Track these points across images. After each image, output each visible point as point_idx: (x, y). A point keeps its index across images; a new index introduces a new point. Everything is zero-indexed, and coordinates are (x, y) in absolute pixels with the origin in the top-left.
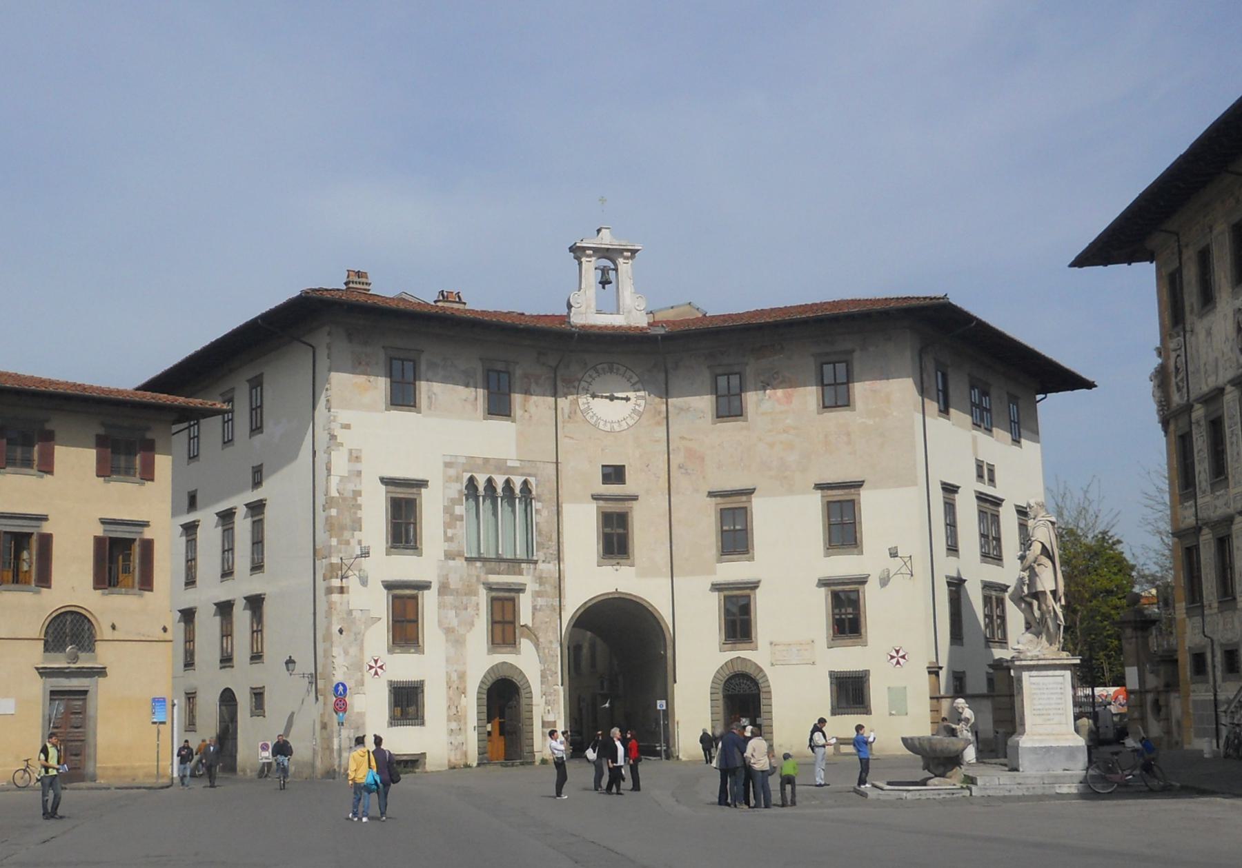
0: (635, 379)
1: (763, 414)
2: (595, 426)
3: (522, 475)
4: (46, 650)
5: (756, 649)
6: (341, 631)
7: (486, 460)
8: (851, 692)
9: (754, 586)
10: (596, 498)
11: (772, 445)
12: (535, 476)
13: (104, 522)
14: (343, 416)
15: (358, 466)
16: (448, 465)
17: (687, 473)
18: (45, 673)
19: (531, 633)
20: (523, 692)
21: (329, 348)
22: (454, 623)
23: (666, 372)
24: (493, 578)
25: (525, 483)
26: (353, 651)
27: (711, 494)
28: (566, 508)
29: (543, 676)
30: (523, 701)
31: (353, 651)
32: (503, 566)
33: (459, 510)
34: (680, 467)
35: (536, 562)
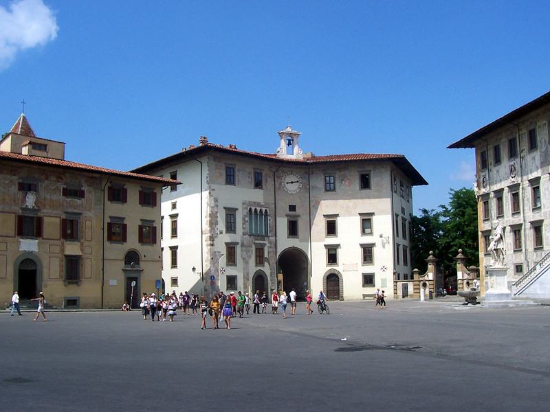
4: (125, 264)
8: (368, 280)
10: (287, 216)
13: (141, 220)
14: (213, 186)
16: (243, 204)
18: (124, 271)
20: (265, 279)
21: (208, 163)
22: (246, 256)
24: (257, 242)
28: (278, 219)
30: (265, 282)
32: (259, 238)
33: (247, 219)
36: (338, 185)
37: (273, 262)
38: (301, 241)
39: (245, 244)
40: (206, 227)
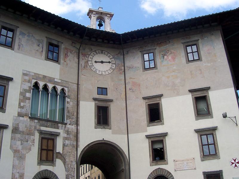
0: (112, 57)
1: (164, 66)
2: (95, 72)
3: (62, 86)
5: (167, 164)
7: (45, 77)
10: (95, 99)
11: (168, 77)
12: (68, 87)
16: (24, 74)
17: (133, 92)
19: (61, 156)
22: (20, 147)
23: (124, 55)
24: (43, 128)
27: (144, 98)
28: (82, 103)
32: (49, 124)
33: (29, 95)
34: (130, 89)
35: (66, 124)
36: (158, 60)
38: (113, 133)
39: (21, 129)
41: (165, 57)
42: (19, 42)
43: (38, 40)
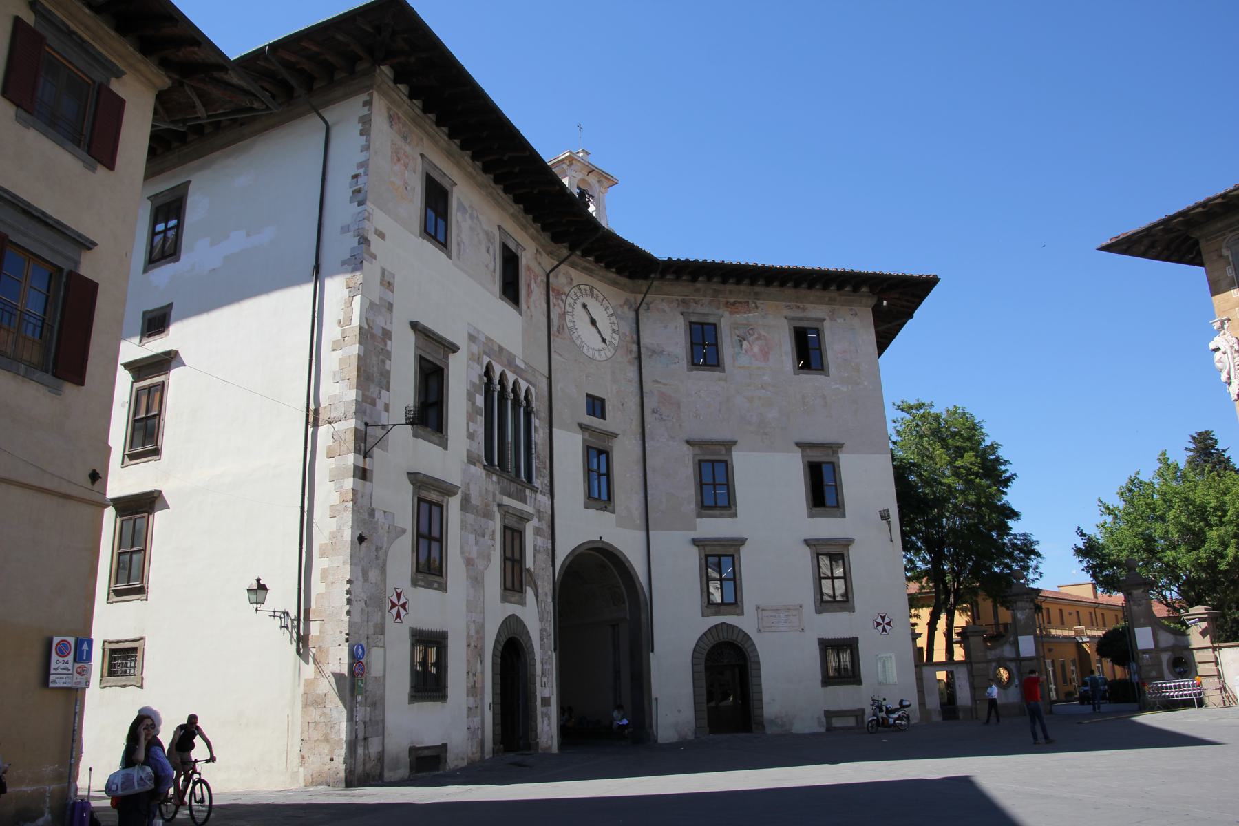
0: (610, 311)
2: (580, 348)
3: (526, 380)
5: (742, 614)
6: (361, 539)
7: (501, 349)
8: (840, 660)
9: (742, 541)
10: (583, 427)
12: (534, 386)
15: (389, 297)
17: (661, 419)
22: (474, 554)
24: (506, 500)
25: (527, 390)
26: (374, 575)
29: (542, 639)
31: (374, 575)
33: (480, 401)
34: (653, 412)
37: (546, 587)
38: (621, 524)
39: (473, 501)
40: (339, 391)
41: (745, 344)
42: (458, 235)
43: (487, 233)
